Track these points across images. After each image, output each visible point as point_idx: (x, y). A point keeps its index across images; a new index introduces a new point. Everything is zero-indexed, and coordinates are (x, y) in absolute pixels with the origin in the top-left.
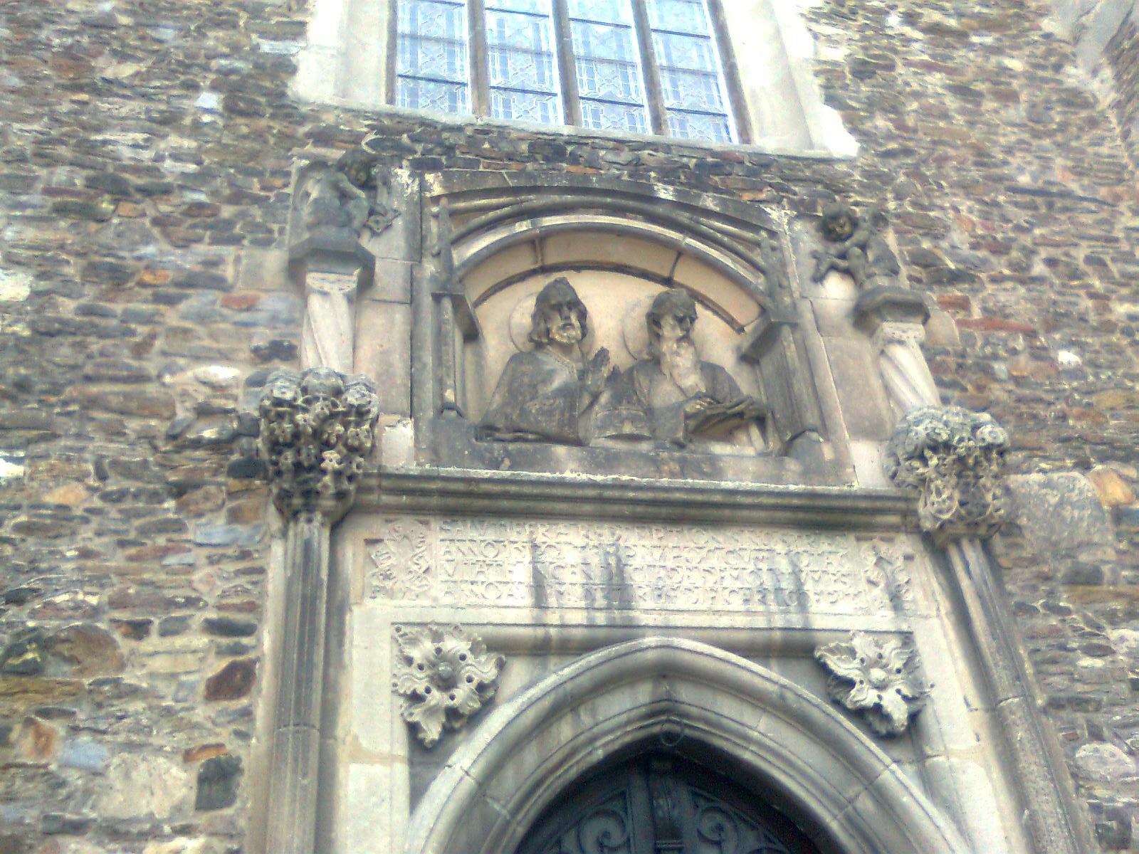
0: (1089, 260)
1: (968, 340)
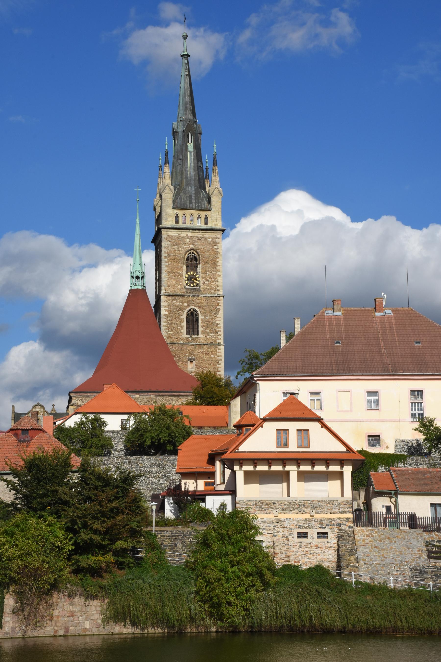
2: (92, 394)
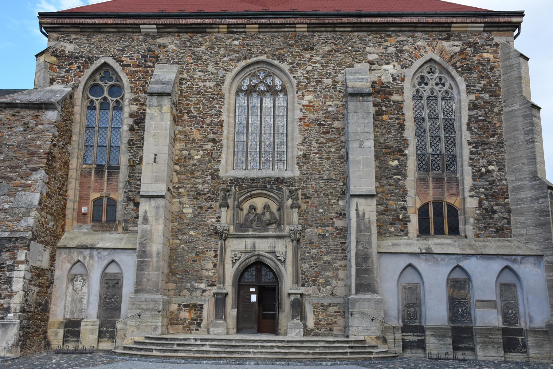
0: (331, 192)
1: (307, 208)
2: (109, 21)
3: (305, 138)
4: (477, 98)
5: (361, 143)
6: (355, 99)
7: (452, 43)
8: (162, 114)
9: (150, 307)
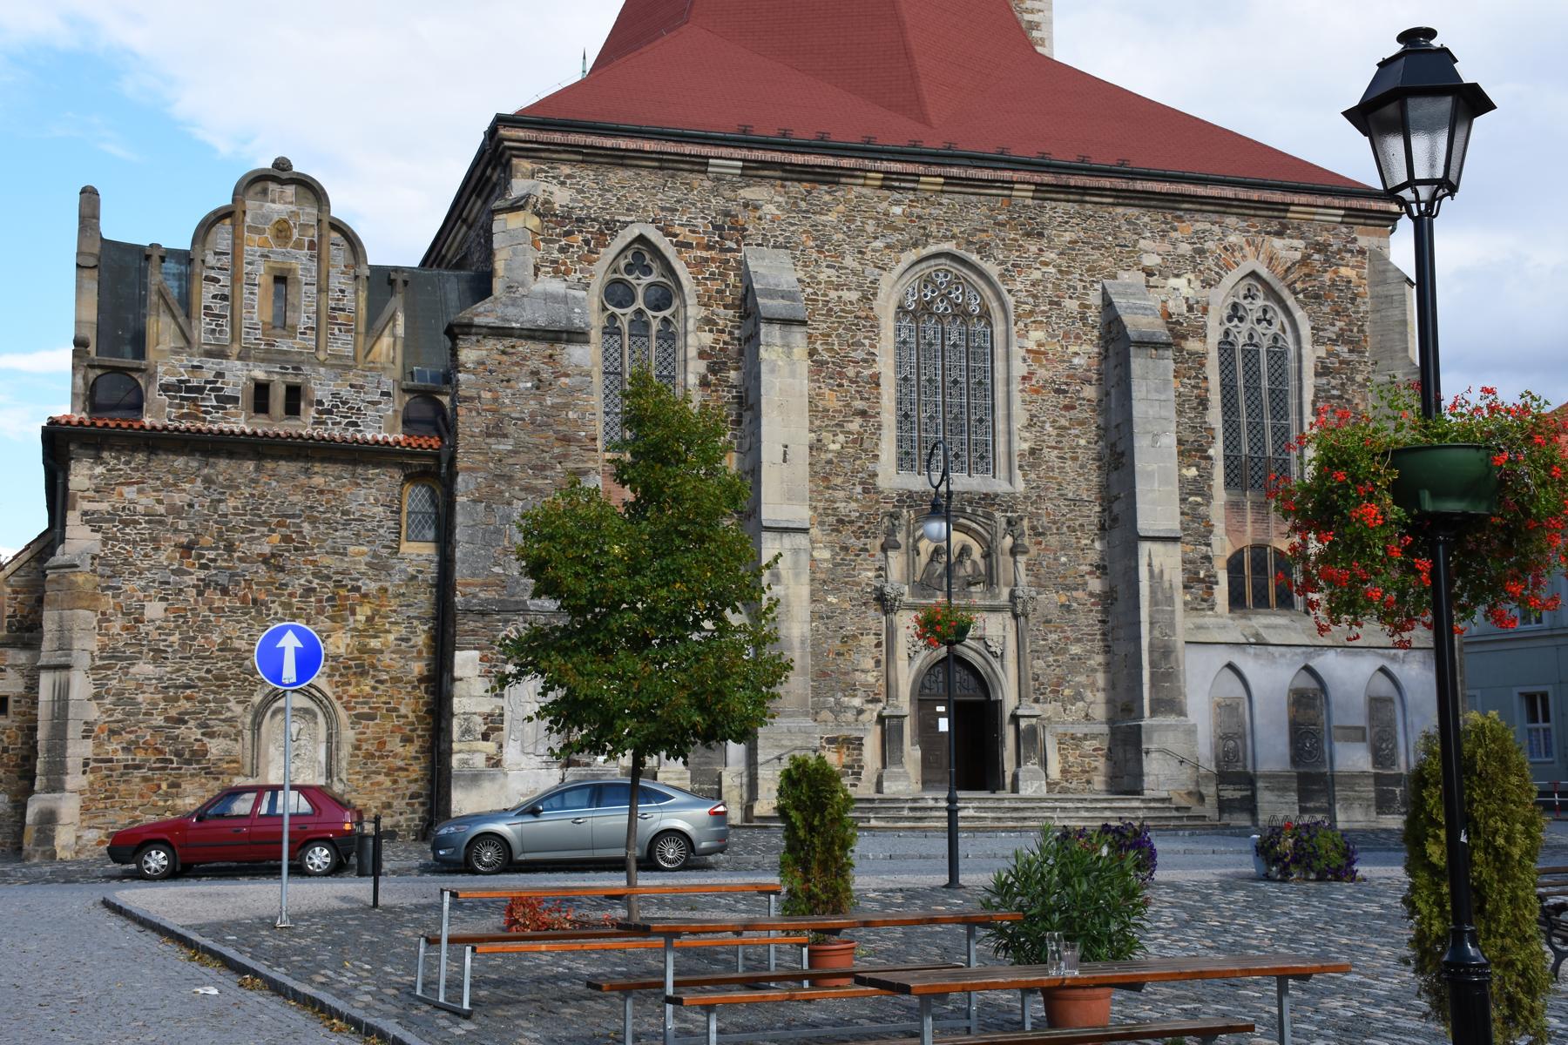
2: (648, 146)
3: (1032, 417)
4: (1330, 354)
5: (1155, 436)
6: (1142, 351)
7: (1287, 241)
8: (792, 363)
9: (799, 743)
